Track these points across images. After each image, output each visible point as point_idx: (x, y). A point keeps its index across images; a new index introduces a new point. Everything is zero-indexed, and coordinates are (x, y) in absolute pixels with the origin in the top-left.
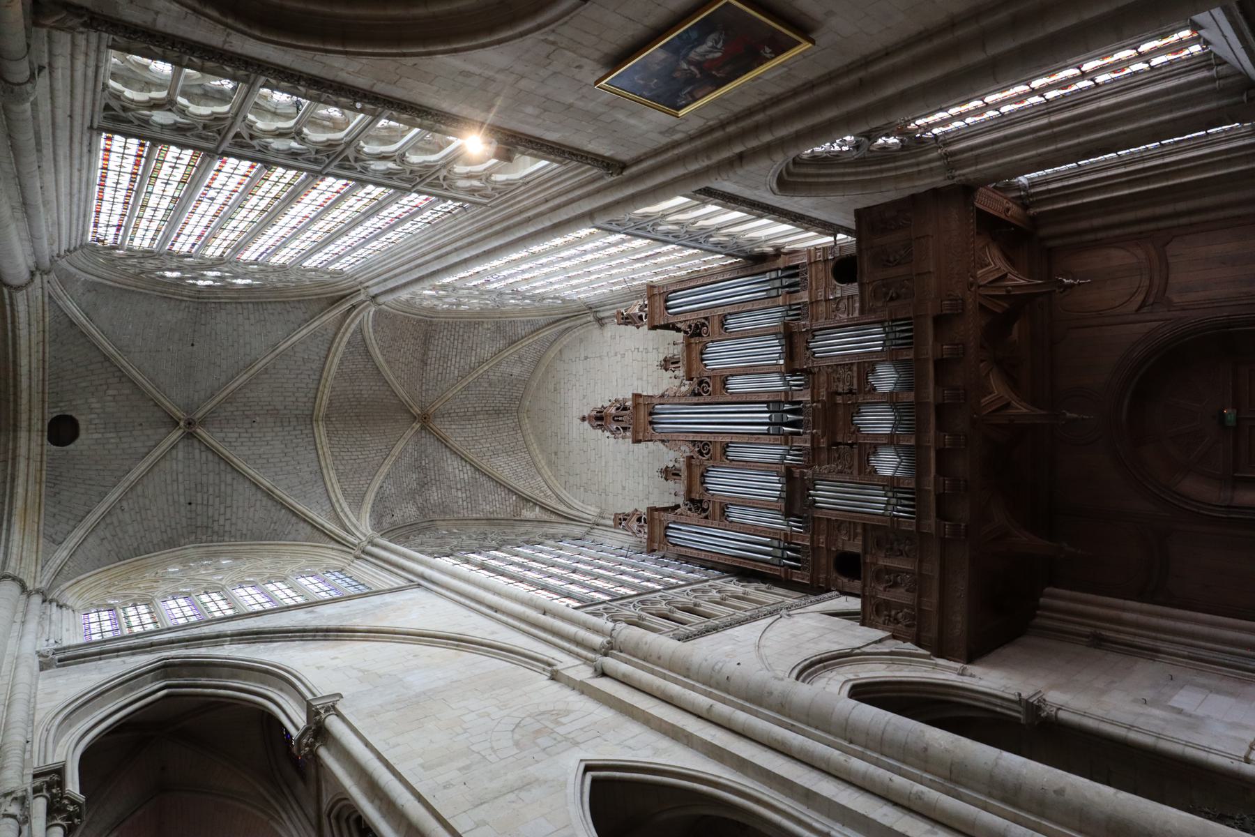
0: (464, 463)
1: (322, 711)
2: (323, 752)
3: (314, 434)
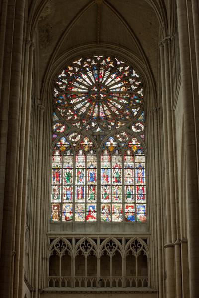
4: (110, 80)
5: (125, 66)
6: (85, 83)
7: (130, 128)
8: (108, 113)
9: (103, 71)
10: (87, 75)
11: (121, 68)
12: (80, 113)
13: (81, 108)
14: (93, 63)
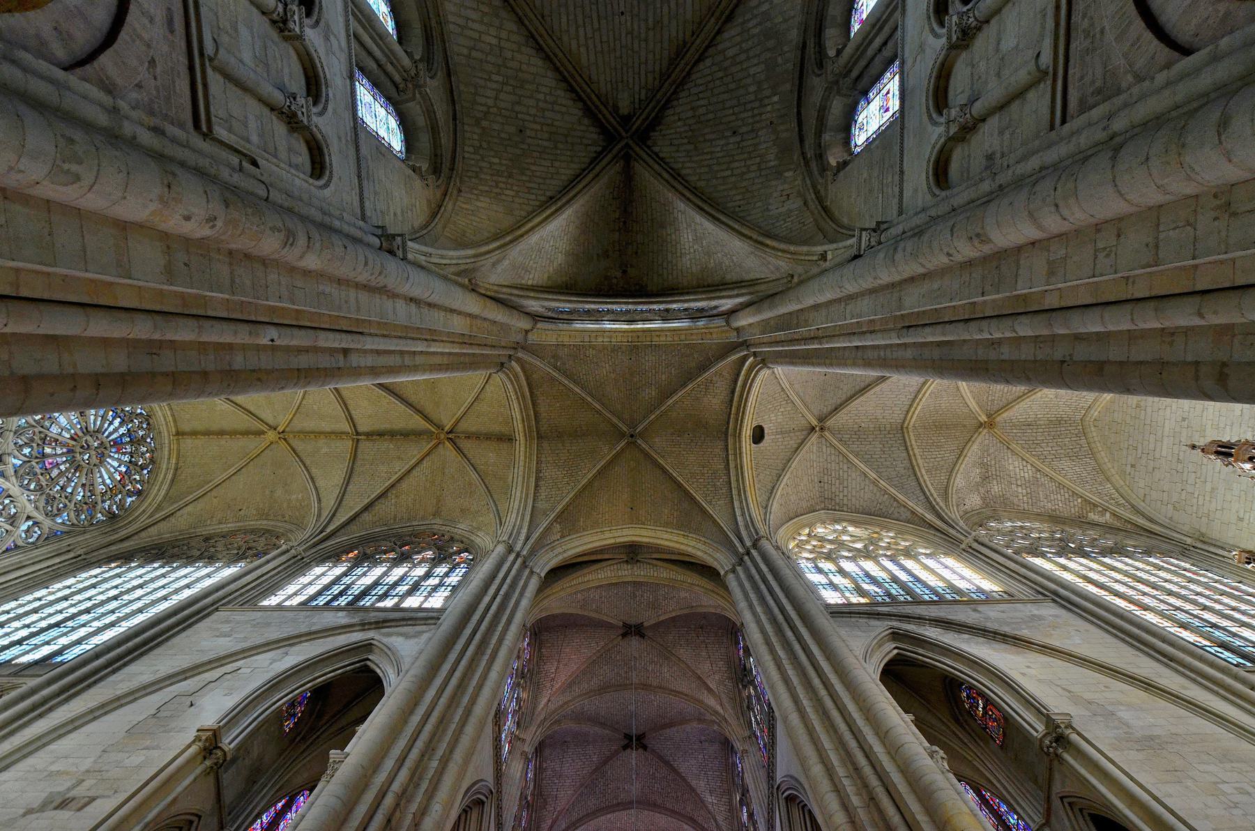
0: (1025, 463)
1: (1062, 726)
2: (1066, 756)
3: (904, 437)
4: (116, 464)
5: (141, 482)
6: (106, 425)
7: (29, 518)
8: (55, 473)
9: (129, 450)
10: (121, 424)
11: (138, 478)
12: (47, 424)
13: (58, 424)
14: (141, 433)
